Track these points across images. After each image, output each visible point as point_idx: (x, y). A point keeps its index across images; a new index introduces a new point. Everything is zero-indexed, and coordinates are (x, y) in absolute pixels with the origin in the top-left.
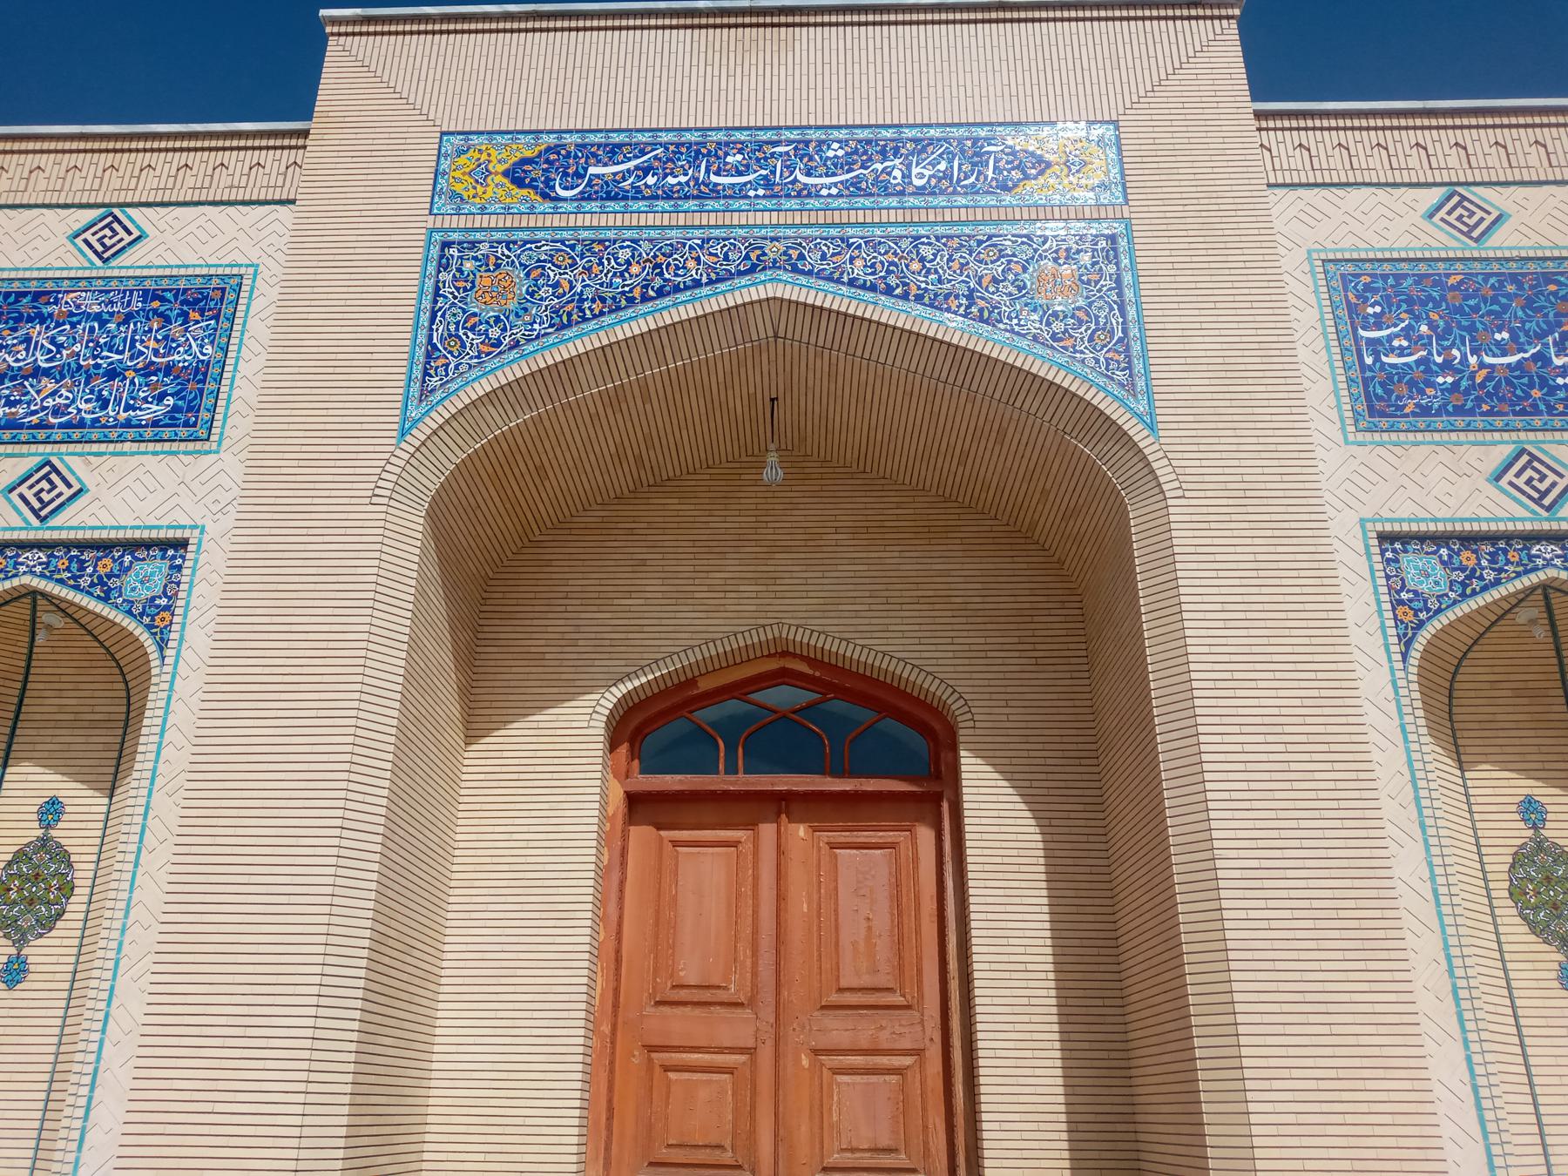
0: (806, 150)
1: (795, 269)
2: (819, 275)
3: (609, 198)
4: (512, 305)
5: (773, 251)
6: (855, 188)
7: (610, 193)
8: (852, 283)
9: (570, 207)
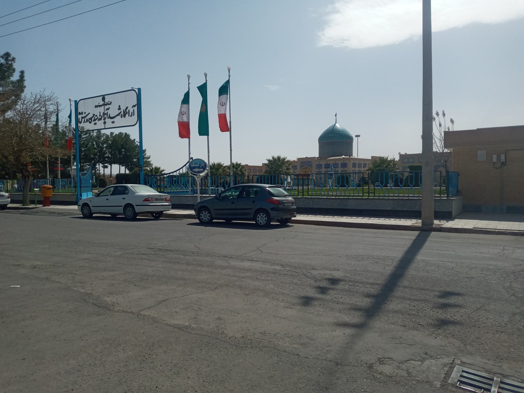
0: (307, 162)
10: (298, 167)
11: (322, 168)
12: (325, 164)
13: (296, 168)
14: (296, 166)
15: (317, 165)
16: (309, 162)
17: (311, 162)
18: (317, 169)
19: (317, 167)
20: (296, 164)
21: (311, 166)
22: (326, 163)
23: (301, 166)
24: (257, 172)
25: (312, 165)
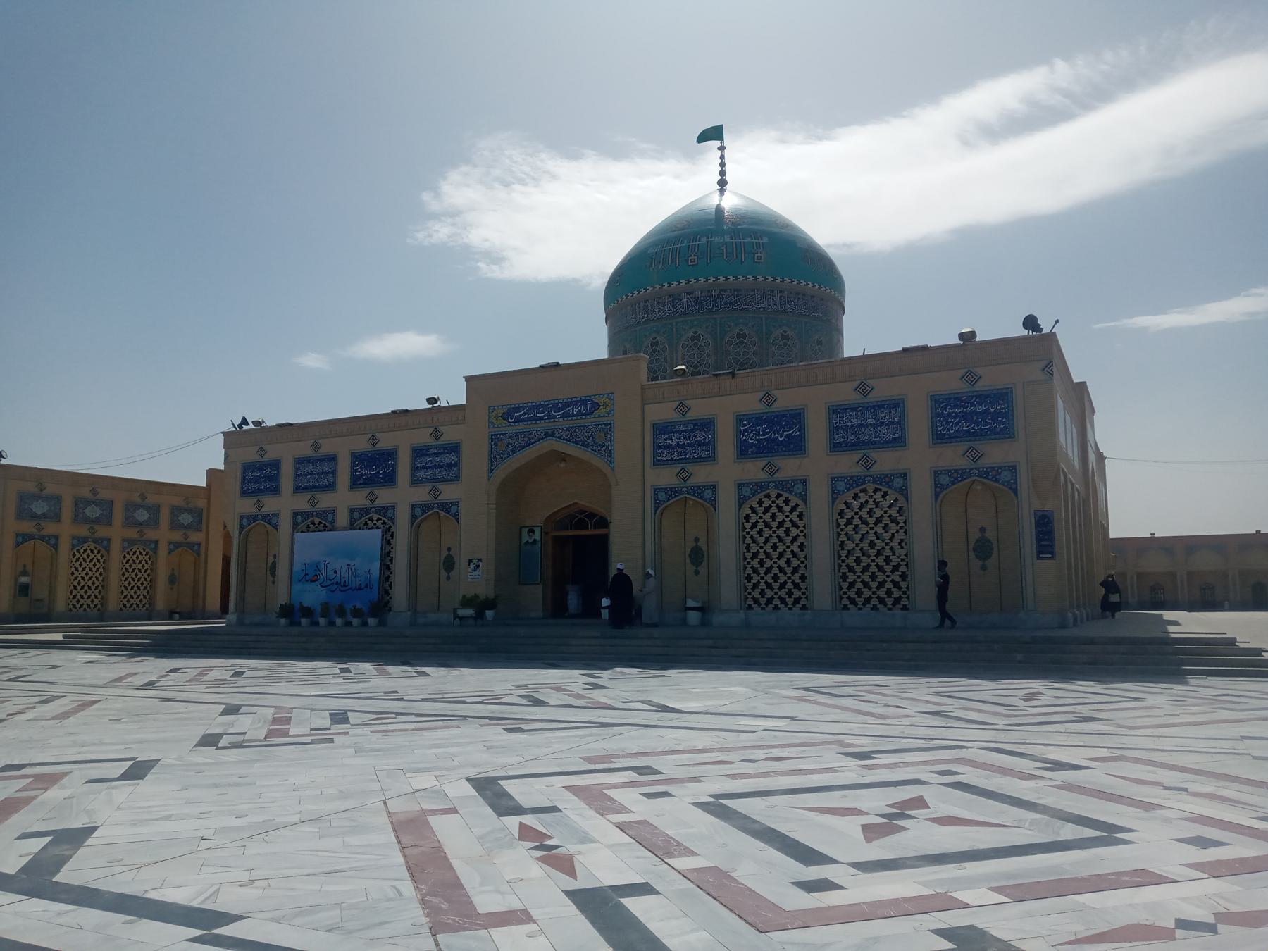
1: (554, 437)
2: (558, 438)
3: (519, 422)
4: (504, 449)
5: (550, 432)
6: (563, 416)
7: (518, 420)
8: (564, 439)
9: (512, 424)
10: (474, 460)
11: (711, 458)
12: (740, 420)
13: (457, 465)
14: (454, 449)
15: (661, 429)
16: (584, 403)
17: (596, 406)
18: (657, 463)
19: (657, 447)
20: (450, 434)
21: (602, 441)
22: (751, 403)
23: (499, 449)
24: (109, 523)
25: (609, 427)
